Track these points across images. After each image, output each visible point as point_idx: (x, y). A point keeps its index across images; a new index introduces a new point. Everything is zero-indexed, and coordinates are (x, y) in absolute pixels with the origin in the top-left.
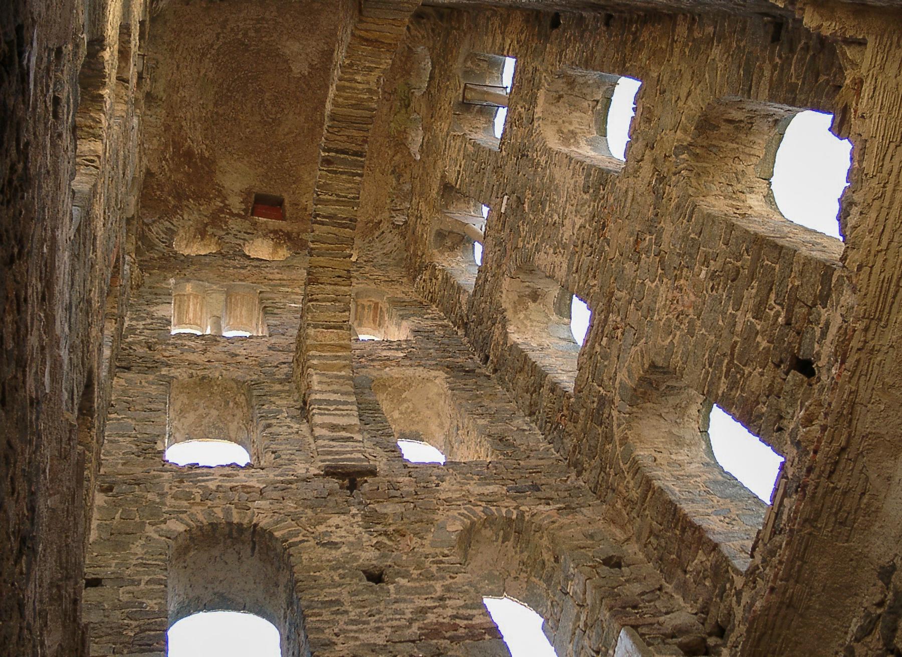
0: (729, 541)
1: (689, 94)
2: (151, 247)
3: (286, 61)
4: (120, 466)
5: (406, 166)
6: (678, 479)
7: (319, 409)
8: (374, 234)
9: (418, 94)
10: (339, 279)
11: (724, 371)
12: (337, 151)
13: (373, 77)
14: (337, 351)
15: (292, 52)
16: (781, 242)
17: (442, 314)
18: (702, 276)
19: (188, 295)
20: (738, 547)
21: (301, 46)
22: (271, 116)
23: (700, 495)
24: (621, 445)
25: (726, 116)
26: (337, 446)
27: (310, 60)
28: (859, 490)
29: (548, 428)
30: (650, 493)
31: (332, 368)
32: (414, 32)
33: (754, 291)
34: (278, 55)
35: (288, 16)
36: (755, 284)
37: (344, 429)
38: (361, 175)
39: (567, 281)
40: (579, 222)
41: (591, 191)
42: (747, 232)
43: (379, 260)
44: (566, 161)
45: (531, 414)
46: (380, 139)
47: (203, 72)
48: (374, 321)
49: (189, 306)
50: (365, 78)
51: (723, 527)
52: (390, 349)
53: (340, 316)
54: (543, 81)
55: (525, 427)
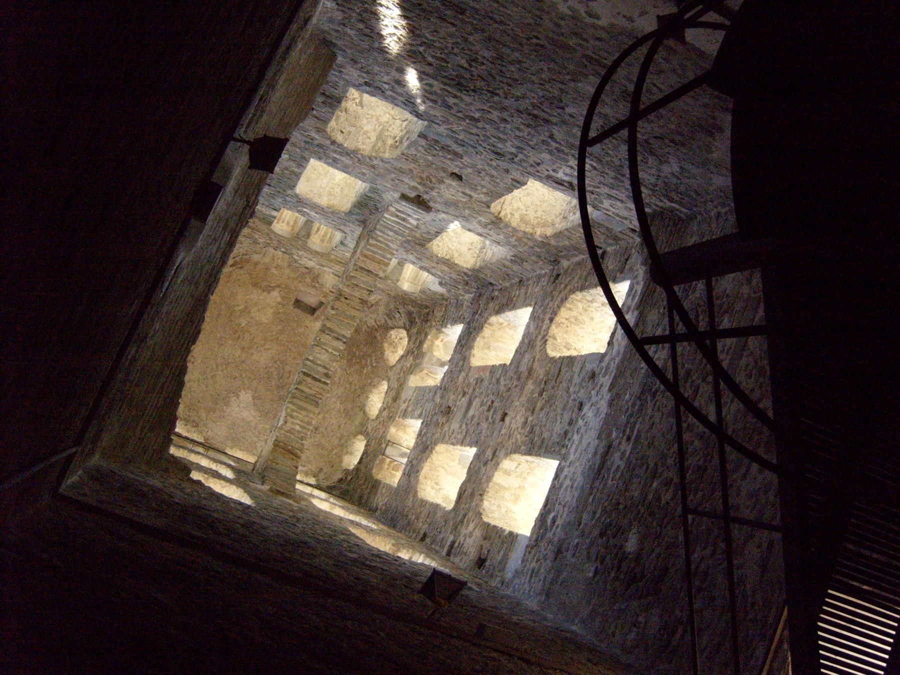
2: (410, 314)
3: (255, 404)
4: (540, 263)
7: (405, 232)
8: (240, 259)
12: (319, 381)
13: (289, 425)
14: (371, 255)
15: (249, 411)
19: (408, 281)
21: (242, 414)
26: (410, 212)
31: (380, 248)
37: (397, 216)
38: (308, 359)
49: (410, 274)
53: (358, 275)
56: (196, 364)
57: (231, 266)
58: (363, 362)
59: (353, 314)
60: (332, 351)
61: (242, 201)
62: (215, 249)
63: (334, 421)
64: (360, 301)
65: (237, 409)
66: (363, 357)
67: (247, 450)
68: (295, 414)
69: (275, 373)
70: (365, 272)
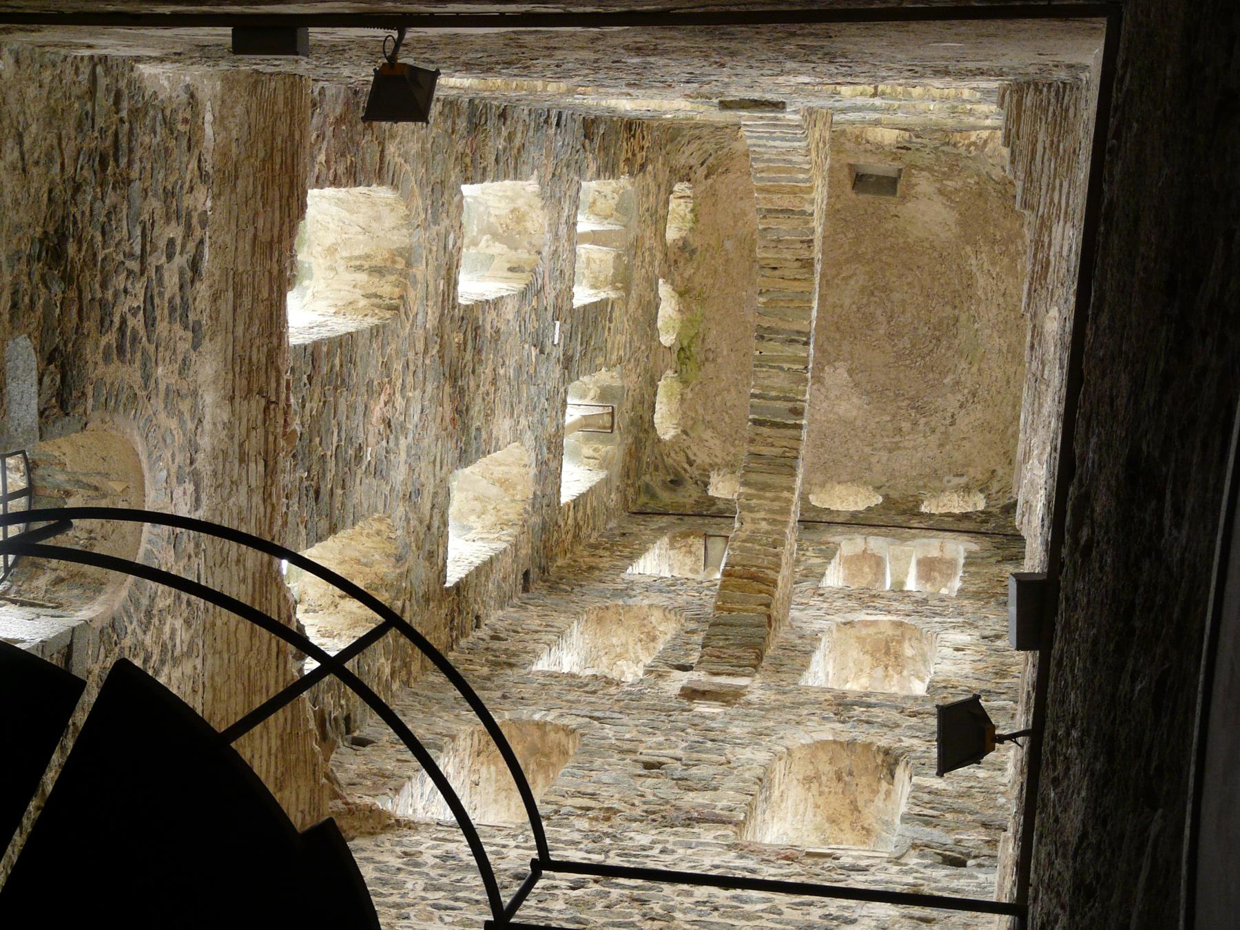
3: (857, 385)
5: (676, 262)
9: (670, 373)
12: (785, 426)
13: (748, 526)
21: (836, 409)
22: (877, 299)
24: (412, 191)
27: (823, 390)
28: (237, 400)
31: (779, 170)
32: (681, 458)
34: (868, 393)
35: (856, 458)
38: (753, 396)
46: (716, 293)
47: (974, 369)
50: (757, 526)
53: (772, 222)
56: (720, 360)
57: (707, 177)
58: (1012, 248)
60: (789, 366)
61: (254, 404)
62: (241, 498)
63: (998, 373)
64: (798, 264)
65: (825, 405)
66: (1011, 240)
67: (855, 479)
68: (754, 502)
69: (879, 312)
70: (781, 216)
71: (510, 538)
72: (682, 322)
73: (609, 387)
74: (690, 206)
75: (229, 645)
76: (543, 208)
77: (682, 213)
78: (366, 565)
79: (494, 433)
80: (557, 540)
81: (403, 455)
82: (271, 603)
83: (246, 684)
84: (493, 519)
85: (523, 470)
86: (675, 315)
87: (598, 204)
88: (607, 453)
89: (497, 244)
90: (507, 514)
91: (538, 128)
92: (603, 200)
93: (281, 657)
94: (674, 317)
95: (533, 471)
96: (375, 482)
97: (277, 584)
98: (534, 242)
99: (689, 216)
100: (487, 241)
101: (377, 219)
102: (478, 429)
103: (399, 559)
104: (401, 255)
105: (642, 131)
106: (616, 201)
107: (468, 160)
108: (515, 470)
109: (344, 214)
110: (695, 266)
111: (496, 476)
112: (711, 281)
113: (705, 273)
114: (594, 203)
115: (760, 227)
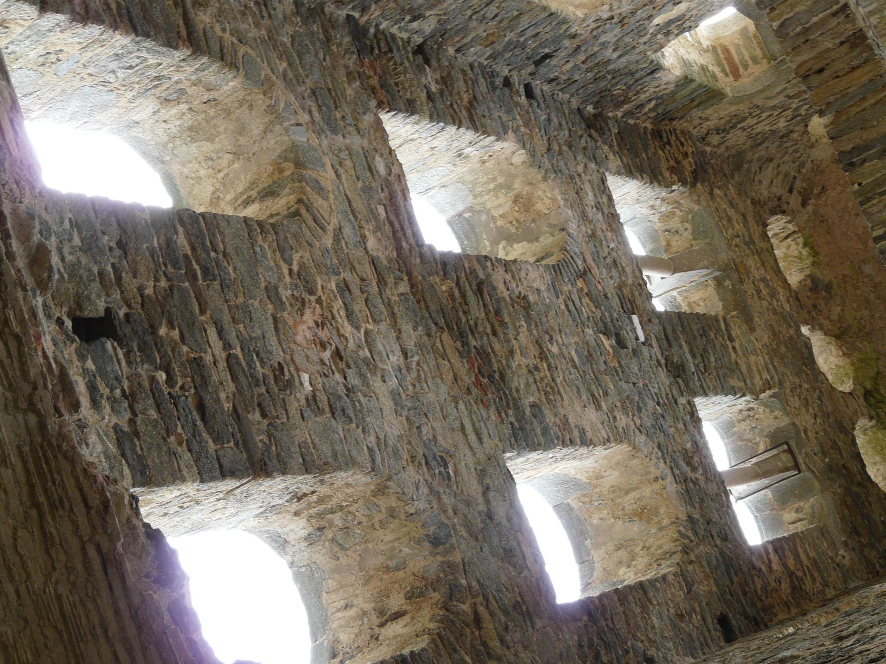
0: (29, 28)
1: (478, 620)
5: (815, 306)
6: (158, 78)
8: (803, 180)
9: (863, 423)
10: (817, 67)
11: (194, 262)
16: (230, 484)
17: (631, 122)
18: (305, 377)
20: (12, 26)
23: (113, 72)
24: (268, 79)
25: (406, 619)
29: (383, 44)
30: (184, 33)
33: (223, 396)
36: (227, 406)
39: (484, 268)
40: (518, 360)
41: (528, 411)
42: (284, 473)
43: (772, 147)
44: (589, 435)
45: (420, 50)
48: (726, 50)
51: (53, 44)
52: (678, 19)
54: (690, 534)
55: (415, 25)
57: (804, 204)
59: (864, 79)
64: (846, 47)
71: (671, 569)
72: (853, 364)
73: (778, 431)
74: (801, 240)
75: (9, 569)
76: (545, 179)
77: (796, 253)
78: (397, 569)
79: (572, 420)
80: (764, 588)
81: (387, 404)
82: (64, 487)
83: (61, 626)
84: (646, 560)
85: (657, 486)
86: (841, 361)
87: (673, 243)
88: (812, 507)
89: (515, 246)
90: (660, 547)
91: (494, 88)
92: (676, 238)
93: (111, 570)
94: (841, 364)
95: (672, 487)
96: (339, 427)
97: (65, 456)
98: (552, 221)
99: (805, 252)
100: (504, 248)
101: (241, 130)
102: (533, 406)
103: (436, 542)
104: (286, 159)
105: (677, 138)
106: (690, 231)
107: (375, 82)
108: (647, 491)
109: (207, 147)
110: (838, 301)
111: (629, 508)
112: (866, 313)
113: (855, 305)
114: (669, 245)
115: (775, 25)
